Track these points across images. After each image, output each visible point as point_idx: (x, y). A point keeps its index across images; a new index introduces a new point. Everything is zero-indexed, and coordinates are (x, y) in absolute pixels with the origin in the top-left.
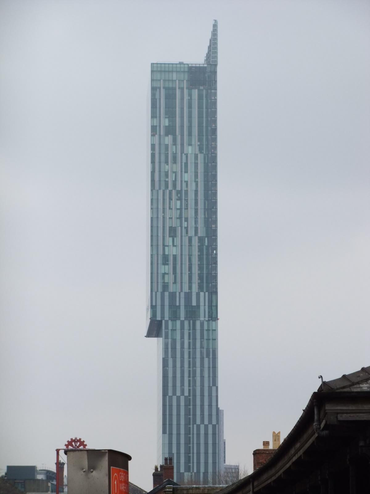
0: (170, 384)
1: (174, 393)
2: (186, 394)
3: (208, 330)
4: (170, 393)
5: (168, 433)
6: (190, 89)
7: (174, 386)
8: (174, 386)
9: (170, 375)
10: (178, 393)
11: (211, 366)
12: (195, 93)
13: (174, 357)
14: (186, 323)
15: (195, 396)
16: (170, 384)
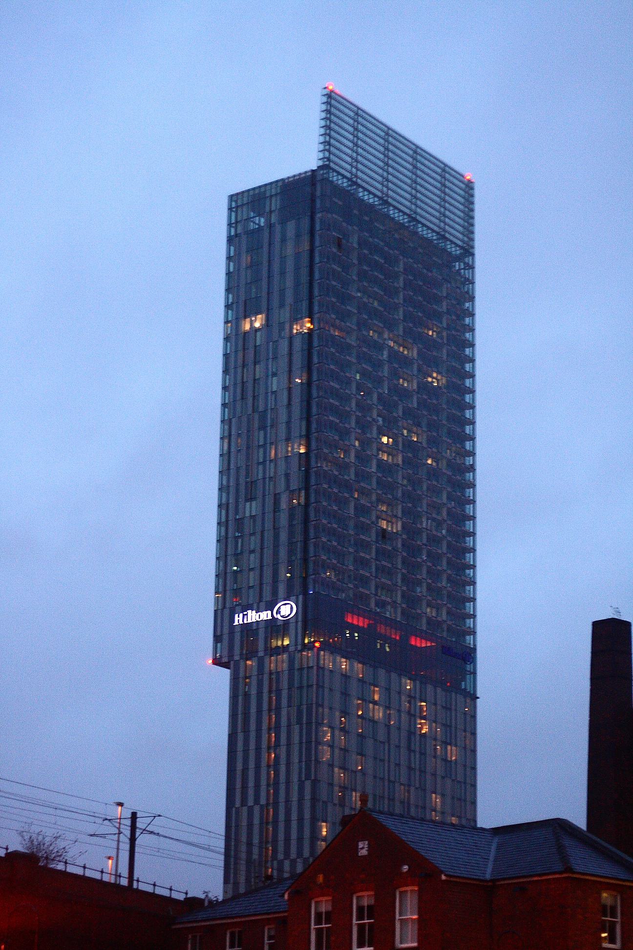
0: (238, 785)
1: (244, 802)
2: (263, 801)
3: (301, 669)
4: (238, 804)
5: (232, 881)
6: (283, 222)
7: (244, 787)
8: (244, 787)
9: (239, 766)
10: (251, 802)
11: (304, 741)
12: (291, 226)
13: (246, 731)
14: (267, 660)
15: (276, 804)
16: (238, 785)
